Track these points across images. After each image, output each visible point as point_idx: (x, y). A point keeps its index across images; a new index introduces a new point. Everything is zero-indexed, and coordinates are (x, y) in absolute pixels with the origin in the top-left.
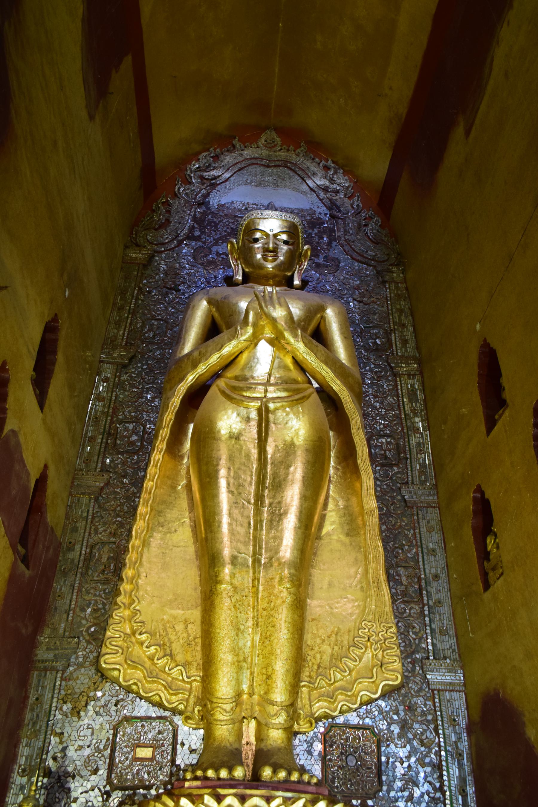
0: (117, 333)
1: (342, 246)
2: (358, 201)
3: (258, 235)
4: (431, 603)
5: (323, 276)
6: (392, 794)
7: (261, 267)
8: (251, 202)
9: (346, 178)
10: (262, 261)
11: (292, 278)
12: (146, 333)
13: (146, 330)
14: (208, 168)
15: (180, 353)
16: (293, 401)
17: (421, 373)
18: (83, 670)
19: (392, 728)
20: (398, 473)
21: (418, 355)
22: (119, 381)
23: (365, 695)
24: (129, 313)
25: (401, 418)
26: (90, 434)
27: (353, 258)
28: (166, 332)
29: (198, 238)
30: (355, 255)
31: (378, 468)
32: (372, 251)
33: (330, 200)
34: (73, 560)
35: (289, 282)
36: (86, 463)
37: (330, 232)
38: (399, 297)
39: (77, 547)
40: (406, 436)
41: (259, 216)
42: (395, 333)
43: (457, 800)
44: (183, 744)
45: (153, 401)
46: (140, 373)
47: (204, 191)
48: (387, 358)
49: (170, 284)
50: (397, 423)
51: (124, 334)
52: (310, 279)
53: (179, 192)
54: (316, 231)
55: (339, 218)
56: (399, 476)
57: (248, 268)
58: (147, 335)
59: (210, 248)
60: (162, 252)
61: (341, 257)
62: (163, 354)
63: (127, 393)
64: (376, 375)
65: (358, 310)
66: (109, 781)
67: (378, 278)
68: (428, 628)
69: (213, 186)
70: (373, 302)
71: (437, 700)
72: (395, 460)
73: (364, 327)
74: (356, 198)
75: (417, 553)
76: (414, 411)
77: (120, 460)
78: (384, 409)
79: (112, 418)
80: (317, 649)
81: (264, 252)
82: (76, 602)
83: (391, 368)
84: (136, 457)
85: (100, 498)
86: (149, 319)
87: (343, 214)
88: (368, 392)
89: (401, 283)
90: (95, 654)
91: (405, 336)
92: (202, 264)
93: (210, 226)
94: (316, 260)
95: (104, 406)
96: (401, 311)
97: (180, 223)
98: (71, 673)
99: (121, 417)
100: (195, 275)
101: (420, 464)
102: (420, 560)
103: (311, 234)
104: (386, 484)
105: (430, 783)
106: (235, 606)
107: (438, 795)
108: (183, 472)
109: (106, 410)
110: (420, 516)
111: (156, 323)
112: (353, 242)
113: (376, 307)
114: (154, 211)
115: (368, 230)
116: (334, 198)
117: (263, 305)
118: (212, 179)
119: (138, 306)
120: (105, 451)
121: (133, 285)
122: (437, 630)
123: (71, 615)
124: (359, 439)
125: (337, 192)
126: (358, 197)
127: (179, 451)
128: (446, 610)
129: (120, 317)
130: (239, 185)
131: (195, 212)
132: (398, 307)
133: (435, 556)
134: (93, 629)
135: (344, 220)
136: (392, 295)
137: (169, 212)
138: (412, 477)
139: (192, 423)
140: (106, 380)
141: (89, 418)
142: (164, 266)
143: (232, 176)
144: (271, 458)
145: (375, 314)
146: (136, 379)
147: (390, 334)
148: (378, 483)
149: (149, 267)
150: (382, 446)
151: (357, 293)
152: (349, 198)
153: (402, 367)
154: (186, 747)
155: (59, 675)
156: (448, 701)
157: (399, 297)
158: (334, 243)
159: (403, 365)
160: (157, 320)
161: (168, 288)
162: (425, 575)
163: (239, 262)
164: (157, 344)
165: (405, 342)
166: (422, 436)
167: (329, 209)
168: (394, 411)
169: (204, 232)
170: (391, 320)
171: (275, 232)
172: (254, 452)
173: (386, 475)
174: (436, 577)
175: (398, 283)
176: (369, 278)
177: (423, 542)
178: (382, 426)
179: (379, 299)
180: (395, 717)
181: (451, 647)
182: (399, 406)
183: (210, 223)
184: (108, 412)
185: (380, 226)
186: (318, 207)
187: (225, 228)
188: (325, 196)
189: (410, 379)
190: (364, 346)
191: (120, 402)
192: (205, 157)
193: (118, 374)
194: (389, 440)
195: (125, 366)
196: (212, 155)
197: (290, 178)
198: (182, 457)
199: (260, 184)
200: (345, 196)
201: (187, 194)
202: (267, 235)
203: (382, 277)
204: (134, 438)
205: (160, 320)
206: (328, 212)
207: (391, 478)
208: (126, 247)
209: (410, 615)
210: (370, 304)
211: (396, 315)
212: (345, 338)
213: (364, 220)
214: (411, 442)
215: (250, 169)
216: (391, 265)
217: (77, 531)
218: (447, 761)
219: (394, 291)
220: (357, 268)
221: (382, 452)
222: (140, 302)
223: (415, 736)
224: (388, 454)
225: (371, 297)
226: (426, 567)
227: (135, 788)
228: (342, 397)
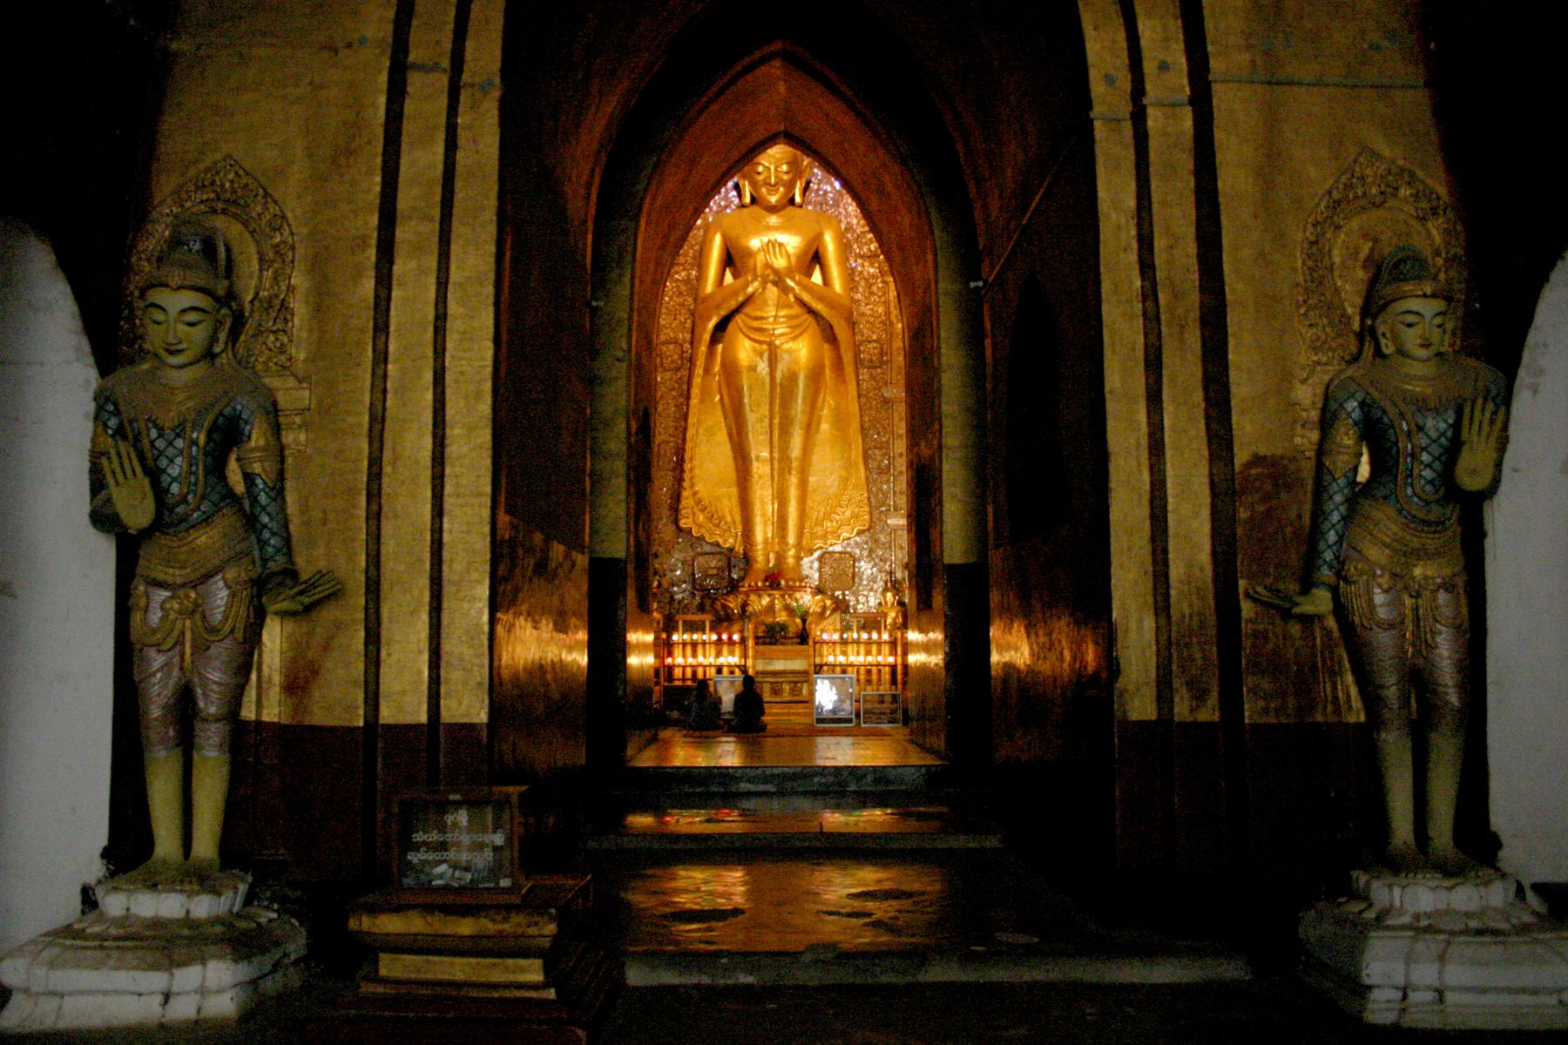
11: (792, 201)
23: (845, 535)
108: (715, 387)
124: (848, 358)
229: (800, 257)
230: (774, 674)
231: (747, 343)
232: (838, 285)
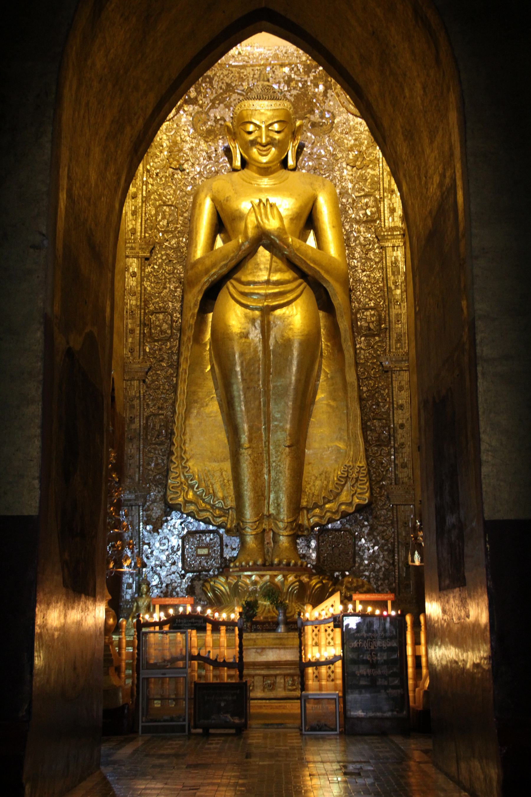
0: (136, 224)
4: (396, 446)
6: (362, 568)
12: (160, 221)
13: (160, 217)
15: (194, 256)
18: (155, 504)
19: (363, 530)
20: (379, 341)
24: (143, 202)
26: (130, 326)
27: (348, 111)
31: (363, 339)
34: (135, 429)
36: (131, 352)
39: (137, 420)
42: (384, 201)
43: (403, 570)
44: (227, 546)
45: (176, 291)
50: (381, 296)
54: (312, 75)
58: (161, 223)
59: (207, 113)
62: (178, 243)
63: (153, 285)
65: (350, 178)
66: (183, 568)
68: (393, 464)
71: (395, 511)
72: (377, 331)
75: (389, 408)
76: (395, 283)
79: (145, 310)
80: (312, 483)
82: (143, 459)
84: (168, 344)
85: (147, 380)
86: (160, 205)
88: (357, 267)
90: (162, 494)
93: (205, 82)
94: (312, 118)
95: (136, 300)
98: (148, 506)
99: (151, 309)
101: (397, 333)
102: (391, 413)
103: (306, 81)
104: (369, 353)
105: (386, 561)
106: (253, 461)
107: (391, 567)
108: (208, 357)
109: (139, 303)
110: (394, 379)
111: (167, 210)
122: (399, 465)
123: (141, 469)
124: (344, 324)
127: (203, 340)
128: (407, 450)
133: (402, 410)
134: (157, 477)
139: (210, 312)
141: (127, 312)
142: (167, 142)
147: (380, 201)
148: (362, 351)
151: (351, 157)
154: (229, 547)
155: (141, 508)
156: (403, 511)
158: (329, 91)
159: (389, 237)
162: (394, 424)
164: (172, 232)
165: (392, 211)
166: (401, 308)
170: (381, 187)
172: (260, 348)
173: (369, 345)
174: (402, 426)
177: (395, 399)
180: (366, 523)
181: (408, 476)
187: (220, 84)
194: (373, 312)
195: (147, 259)
198: (205, 345)
205: (171, 205)
207: (373, 347)
209: (381, 455)
212: (333, 227)
214: (391, 313)
217: (134, 408)
218: (398, 547)
221: (367, 325)
222: (150, 186)
223: (378, 534)
224: (371, 326)
226: (395, 419)
227: (200, 571)
229: (295, 218)
230: (268, 665)
231: (239, 310)
232: (333, 248)
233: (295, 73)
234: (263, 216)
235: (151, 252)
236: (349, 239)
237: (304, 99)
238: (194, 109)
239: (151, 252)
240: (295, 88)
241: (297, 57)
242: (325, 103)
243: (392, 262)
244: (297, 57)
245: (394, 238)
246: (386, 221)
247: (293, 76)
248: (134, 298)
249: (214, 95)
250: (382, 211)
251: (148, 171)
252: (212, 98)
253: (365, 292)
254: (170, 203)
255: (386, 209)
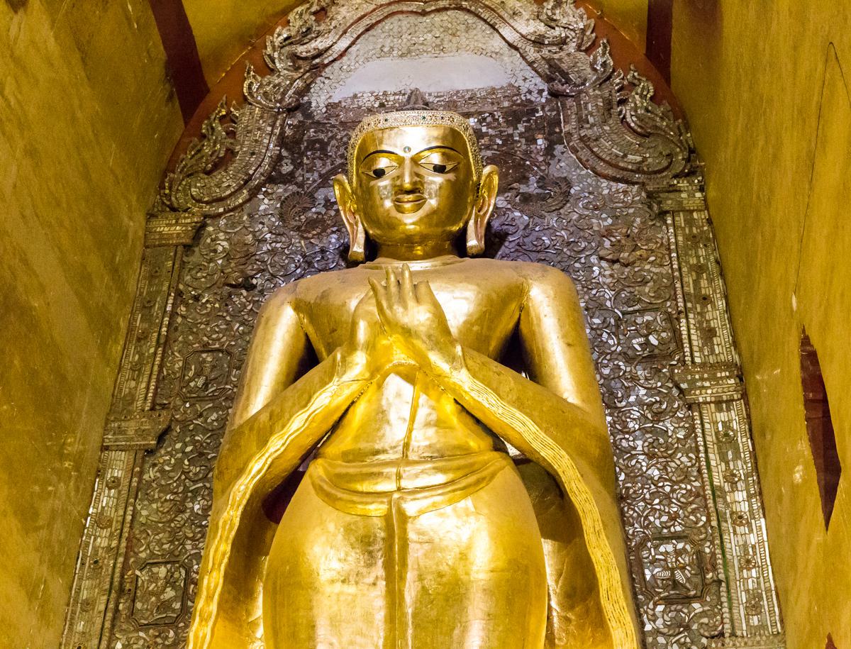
0: (136, 388)
1: (575, 151)
2: (604, 54)
3: (383, 163)
5: (537, 220)
7: (391, 225)
8: (391, 90)
9: (581, 10)
10: (394, 213)
12: (191, 380)
13: (191, 374)
14: (306, 34)
16: (454, 491)
17: (745, 396)
20: (703, 614)
21: (736, 358)
22: (139, 482)
25: (704, 497)
26: (85, 595)
27: (597, 174)
28: (229, 373)
29: (289, 179)
30: (601, 167)
31: (660, 608)
32: (636, 152)
33: (549, 61)
35: (458, 245)
37: (551, 128)
38: (694, 240)
40: (717, 534)
41: (380, 126)
42: (687, 318)
46: (180, 461)
47: (299, 84)
48: (672, 371)
49: (236, 278)
51: (148, 388)
52: (511, 229)
53: (250, 94)
54: (521, 128)
55: (567, 96)
56: (705, 620)
57: (371, 228)
58: (192, 384)
60: (219, 215)
61: (573, 176)
63: (154, 506)
64: (651, 411)
65: (608, 280)
67: (650, 207)
69: (317, 70)
70: (641, 258)
72: (695, 588)
73: (624, 314)
74: (600, 50)
77: (141, 642)
78: (670, 480)
79: (126, 559)
81: (396, 194)
83: (681, 391)
84: (172, 633)
86: (196, 352)
87: (575, 85)
89: (698, 211)
91: (708, 321)
92: (298, 229)
93: (313, 149)
94: (523, 189)
95: (111, 536)
96: (699, 269)
97: (253, 154)
99: (143, 555)
100: (283, 253)
101: (747, 591)
103: (512, 135)
109: (114, 544)
111: (209, 359)
112: (596, 140)
113: (647, 267)
114: (204, 137)
115: (627, 110)
116: (556, 56)
117: (385, 304)
118: (314, 57)
119: (176, 329)
120: (113, 626)
121: (165, 288)
125: (562, 42)
126: (605, 47)
129: (141, 355)
130: (367, 60)
131: (282, 126)
132: (693, 261)
135: (577, 98)
136: (680, 238)
137: (231, 134)
138: (732, 620)
140: (115, 484)
141: (83, 564)
142: (225, 244)
143: (353, 43)
144: (415, 615)
145: (644, 282)
146: (172, 474)
147: (678, 319)
149: (196, 249)
150: (665, 560)
151: (607, 244)
152: (588, 51)
153: (703, 387)
157: (694, 240)
158: (559, 148)
159: (707, 384)
160: (212, 351)
161: (231, 286)
163: (357, 217)
164: (213, 398)
167: (549, 79)
168: (690, 482)
169: (301, 164)
170: (679, 291)
171: (413, 153)
175: (691, 212)
176: (631, 211)
178: (665, 518)
179: (652, 251)
182: (699, 471)
183: (312, 143)
184: (118, 547)
185: (651, 98)
186: (525, 79)
188: (538, 55)
189: (720, 410)
190: (623, 354)
191: (143, 524)
192: (301, 15)
193: (137, 469)
194: (680, 546)
195: (150, 452)
196: (313, 9)
197: (468, 29)
198: (254, 625)
199: (409, 52)
200: (579, 48)
201: (265, 94)
202: (401, 161)
203: (659, 203)
204: (170, 593)
205: (218, 350)
206: (544, 86)
207: (687, 628)
208: (151, 216)
210: (634, 263)
211: (689, 280)
212: (569, 345)
213: (619, 91)
215: (387, 25)
216: (676, 176)
219: (683, 229)
220: (606, 192)
221: (668, 574)
222: (179, 320)
224: (679, 576)
225: (636, 248)
228: (560, 471)
233: (488, 125)
234: (394, 299)
235: (161, 438)
236: (612, 394)
237: (506, 162)
238: (285, 190)
239: (161, 438)
240: (488, 147)
241: (492, 103)
242: (549, 164)
243: (717, 433)
244: (492, 103)
245: (718, 384)
246: (697, 354)
247: (484, 129)
248: (105, 533)
249: (329, 167)
250: (685, 336)
251: (179, 294)
252: (324, 171)
253: (657, 501)
254: (217, 346)
255: (692, 331)
